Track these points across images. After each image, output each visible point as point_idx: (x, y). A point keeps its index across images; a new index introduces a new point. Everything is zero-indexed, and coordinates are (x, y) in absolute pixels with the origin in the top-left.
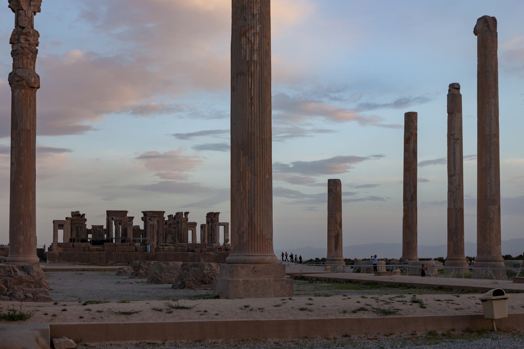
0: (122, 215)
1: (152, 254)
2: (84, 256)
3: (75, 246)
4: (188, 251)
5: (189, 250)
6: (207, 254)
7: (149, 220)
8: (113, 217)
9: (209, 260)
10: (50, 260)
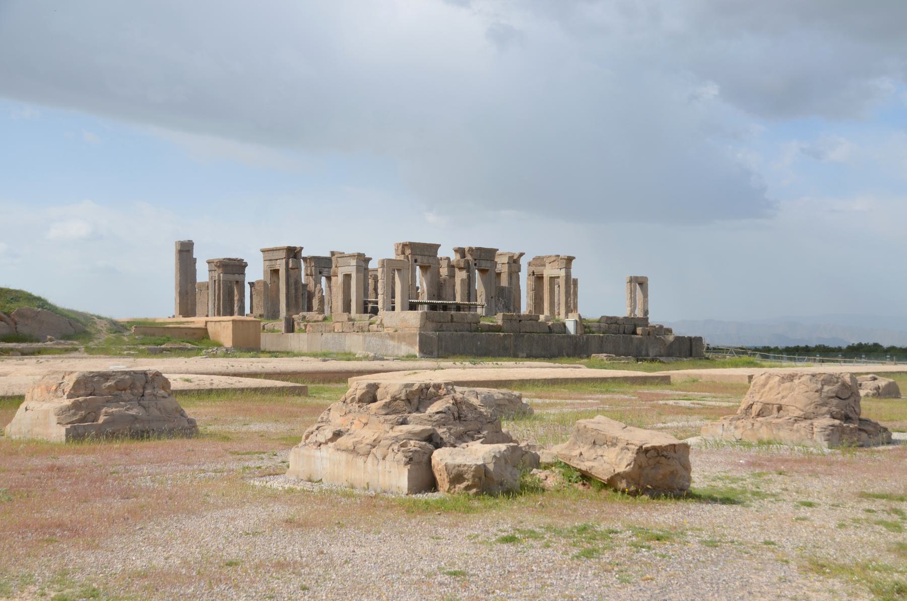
0: (431, 254)
1: (583, 339)
2: (479, 343)
3: (455, 320)
4: (624, 333)
5: (626, 331)
6: (658, 338)
7: (474, 267)
8: (417, 256)
9: (660, 352)
10: (425, 351)
